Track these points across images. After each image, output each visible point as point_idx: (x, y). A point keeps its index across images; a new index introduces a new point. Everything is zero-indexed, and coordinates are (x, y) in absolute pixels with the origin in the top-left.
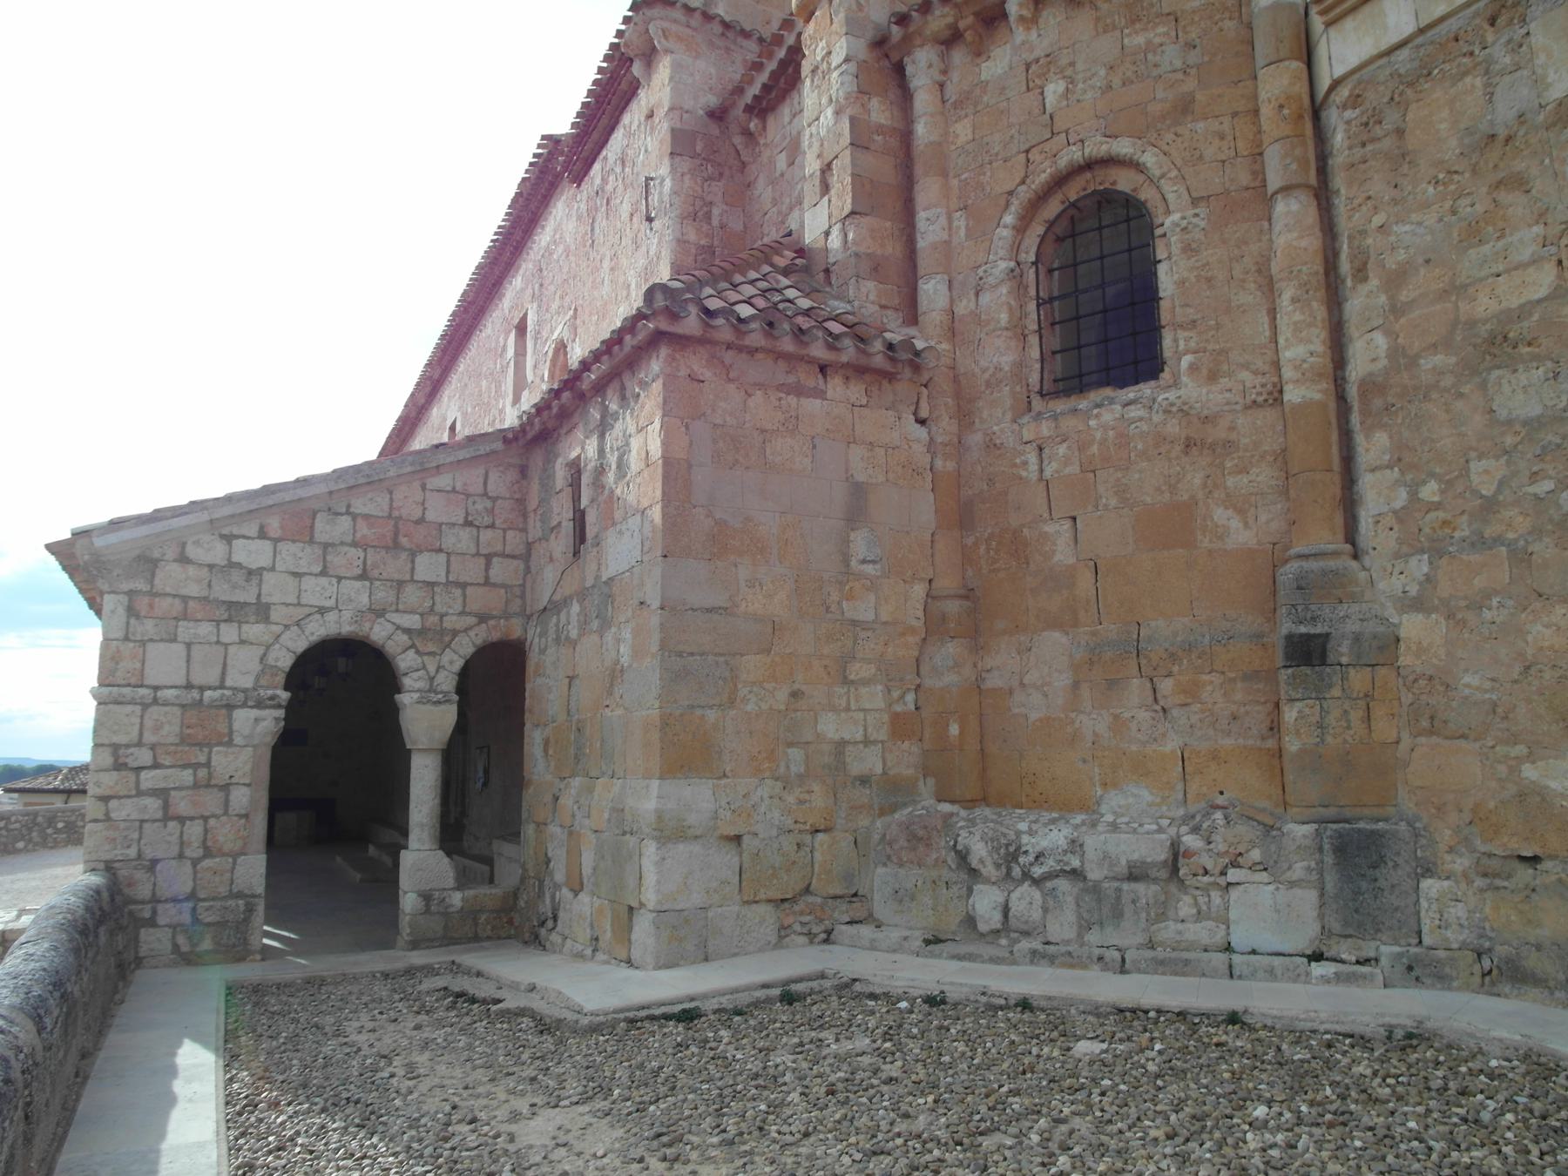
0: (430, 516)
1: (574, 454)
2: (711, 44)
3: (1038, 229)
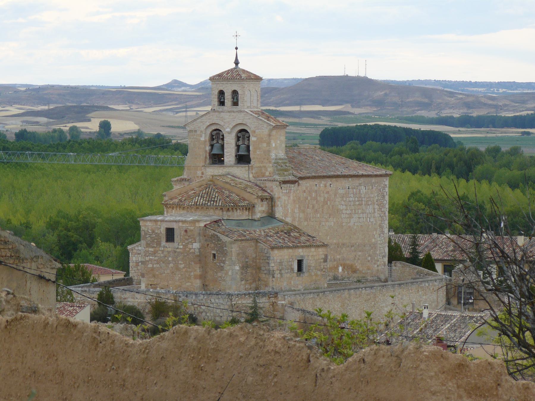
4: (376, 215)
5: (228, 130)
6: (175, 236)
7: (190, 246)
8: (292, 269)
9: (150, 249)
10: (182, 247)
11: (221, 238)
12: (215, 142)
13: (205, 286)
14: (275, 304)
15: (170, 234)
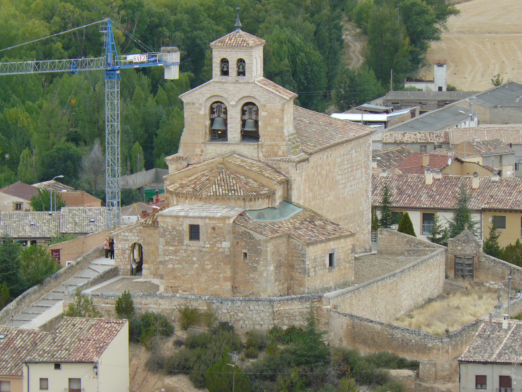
4: (364, 179)
5: (233, 103)
6: (201, 234)
7: (219, 245)
8: (325, 265)
9: (171, 248)
10: (208, 246)
11: (254, 236)
12: (216, 115)
13: (234, 288)
14: (319, 309)
15: (194, 232)
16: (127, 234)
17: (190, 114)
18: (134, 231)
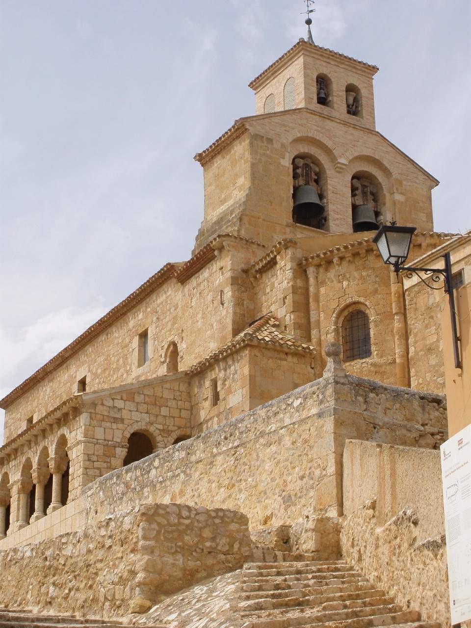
0: (164, 396)
1: (214, 376)
2: (242, 247)
3: (342, 319)
16: (119, 404)
17: (263, 159)
18: (138, 398)
